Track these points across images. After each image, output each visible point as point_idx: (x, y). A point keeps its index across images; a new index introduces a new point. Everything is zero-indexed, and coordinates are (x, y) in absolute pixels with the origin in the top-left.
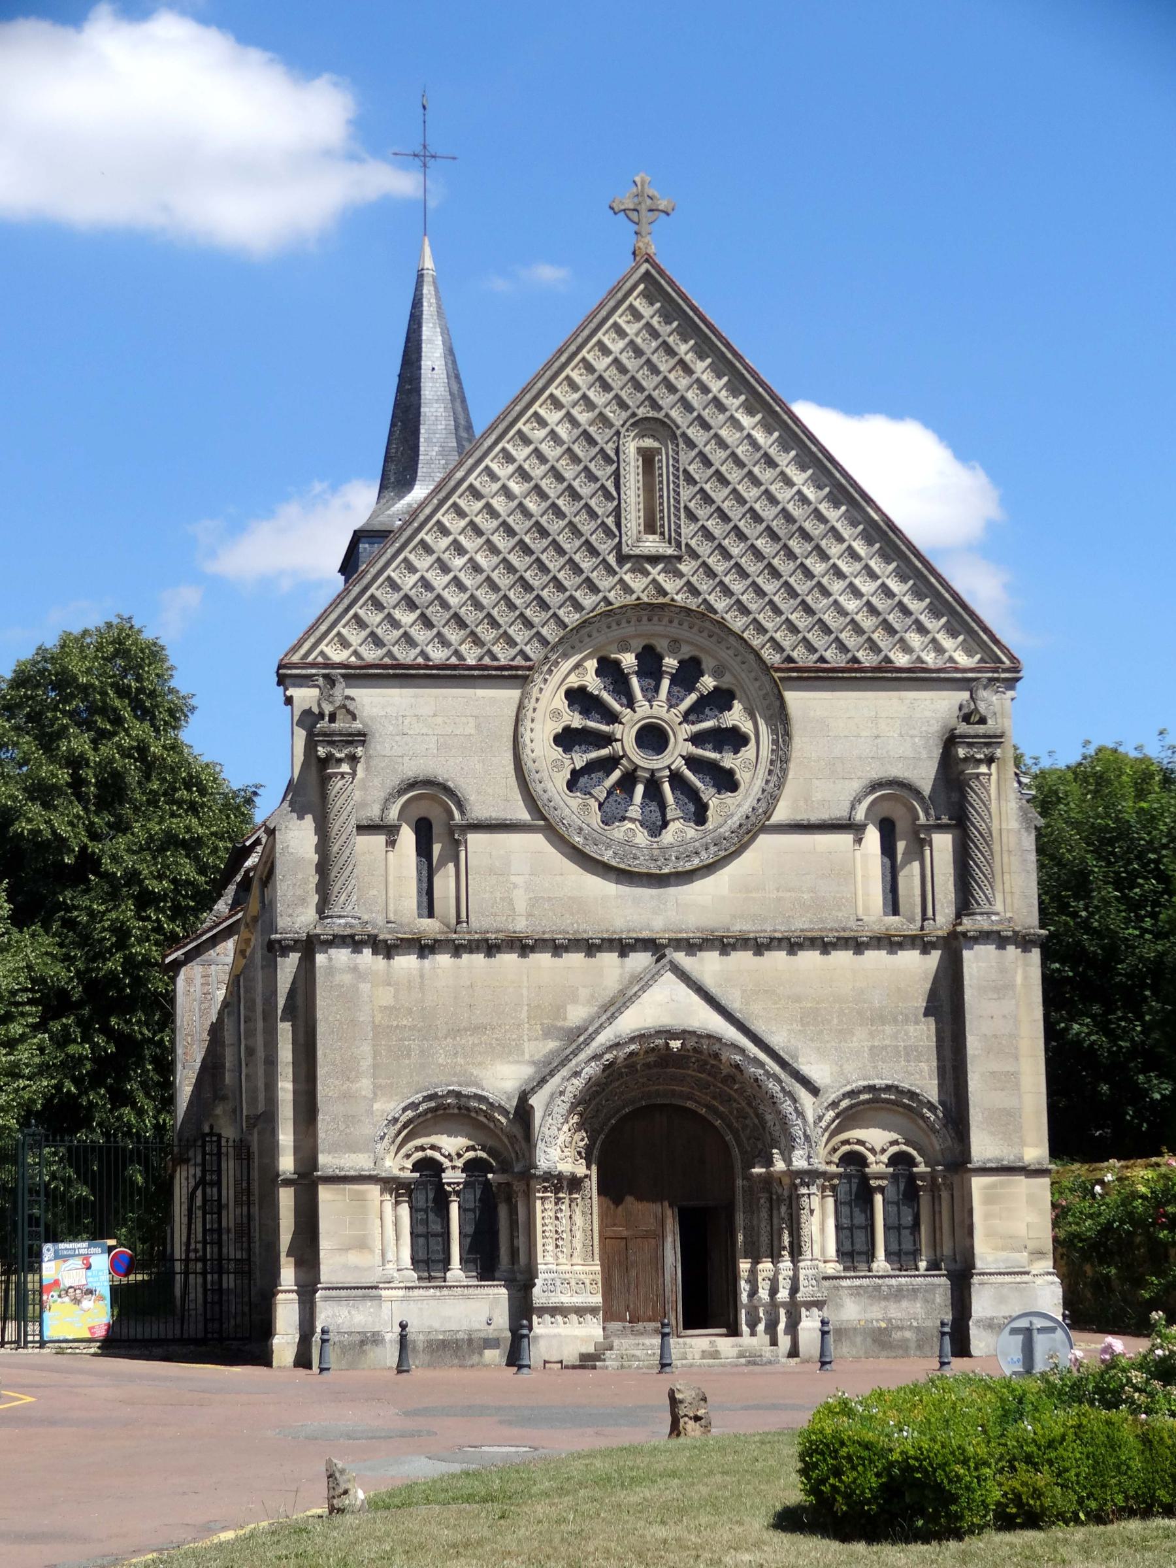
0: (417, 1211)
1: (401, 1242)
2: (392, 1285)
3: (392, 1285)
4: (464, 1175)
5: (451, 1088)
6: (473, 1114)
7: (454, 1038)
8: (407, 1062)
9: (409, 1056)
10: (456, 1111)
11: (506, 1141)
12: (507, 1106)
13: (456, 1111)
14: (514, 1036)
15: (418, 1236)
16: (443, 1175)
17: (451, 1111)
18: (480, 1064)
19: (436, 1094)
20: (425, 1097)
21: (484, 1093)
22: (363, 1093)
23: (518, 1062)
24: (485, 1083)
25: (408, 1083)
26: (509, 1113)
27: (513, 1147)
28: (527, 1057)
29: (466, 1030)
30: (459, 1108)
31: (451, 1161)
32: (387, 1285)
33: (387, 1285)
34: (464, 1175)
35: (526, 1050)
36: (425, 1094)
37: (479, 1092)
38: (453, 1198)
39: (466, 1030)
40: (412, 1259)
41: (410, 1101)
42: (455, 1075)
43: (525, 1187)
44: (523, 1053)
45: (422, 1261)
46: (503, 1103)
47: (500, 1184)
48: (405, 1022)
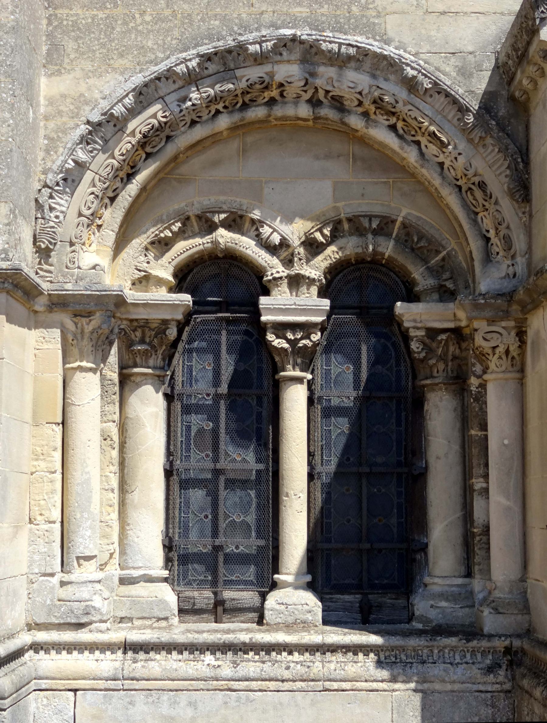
0: (187, 410)
1: (134, 497)
2: (84, 636)
3: (84, 636)
4: (326, 303)
5: (288, 32)
12: (459, 91)
13: (304, 111)
15: (185, 484)
16: (263, 300)
17: (290, 111)
19: (241, 47)
20: (207, 58)
21: (390, 50)
25: (159, 19)
26: (463, 110)
27: (475, 222)
30: (315, 103)
31: (288, 262)
32: (68, 636)
33: (68, 636)
34: (326, 303)
36: (206, 49)
37: (376, 46)
38: (291, 372)
40: (168, 547)
41: (162, 67)
45: (199, 558)
46: (446, 81)
47: (432, 333)
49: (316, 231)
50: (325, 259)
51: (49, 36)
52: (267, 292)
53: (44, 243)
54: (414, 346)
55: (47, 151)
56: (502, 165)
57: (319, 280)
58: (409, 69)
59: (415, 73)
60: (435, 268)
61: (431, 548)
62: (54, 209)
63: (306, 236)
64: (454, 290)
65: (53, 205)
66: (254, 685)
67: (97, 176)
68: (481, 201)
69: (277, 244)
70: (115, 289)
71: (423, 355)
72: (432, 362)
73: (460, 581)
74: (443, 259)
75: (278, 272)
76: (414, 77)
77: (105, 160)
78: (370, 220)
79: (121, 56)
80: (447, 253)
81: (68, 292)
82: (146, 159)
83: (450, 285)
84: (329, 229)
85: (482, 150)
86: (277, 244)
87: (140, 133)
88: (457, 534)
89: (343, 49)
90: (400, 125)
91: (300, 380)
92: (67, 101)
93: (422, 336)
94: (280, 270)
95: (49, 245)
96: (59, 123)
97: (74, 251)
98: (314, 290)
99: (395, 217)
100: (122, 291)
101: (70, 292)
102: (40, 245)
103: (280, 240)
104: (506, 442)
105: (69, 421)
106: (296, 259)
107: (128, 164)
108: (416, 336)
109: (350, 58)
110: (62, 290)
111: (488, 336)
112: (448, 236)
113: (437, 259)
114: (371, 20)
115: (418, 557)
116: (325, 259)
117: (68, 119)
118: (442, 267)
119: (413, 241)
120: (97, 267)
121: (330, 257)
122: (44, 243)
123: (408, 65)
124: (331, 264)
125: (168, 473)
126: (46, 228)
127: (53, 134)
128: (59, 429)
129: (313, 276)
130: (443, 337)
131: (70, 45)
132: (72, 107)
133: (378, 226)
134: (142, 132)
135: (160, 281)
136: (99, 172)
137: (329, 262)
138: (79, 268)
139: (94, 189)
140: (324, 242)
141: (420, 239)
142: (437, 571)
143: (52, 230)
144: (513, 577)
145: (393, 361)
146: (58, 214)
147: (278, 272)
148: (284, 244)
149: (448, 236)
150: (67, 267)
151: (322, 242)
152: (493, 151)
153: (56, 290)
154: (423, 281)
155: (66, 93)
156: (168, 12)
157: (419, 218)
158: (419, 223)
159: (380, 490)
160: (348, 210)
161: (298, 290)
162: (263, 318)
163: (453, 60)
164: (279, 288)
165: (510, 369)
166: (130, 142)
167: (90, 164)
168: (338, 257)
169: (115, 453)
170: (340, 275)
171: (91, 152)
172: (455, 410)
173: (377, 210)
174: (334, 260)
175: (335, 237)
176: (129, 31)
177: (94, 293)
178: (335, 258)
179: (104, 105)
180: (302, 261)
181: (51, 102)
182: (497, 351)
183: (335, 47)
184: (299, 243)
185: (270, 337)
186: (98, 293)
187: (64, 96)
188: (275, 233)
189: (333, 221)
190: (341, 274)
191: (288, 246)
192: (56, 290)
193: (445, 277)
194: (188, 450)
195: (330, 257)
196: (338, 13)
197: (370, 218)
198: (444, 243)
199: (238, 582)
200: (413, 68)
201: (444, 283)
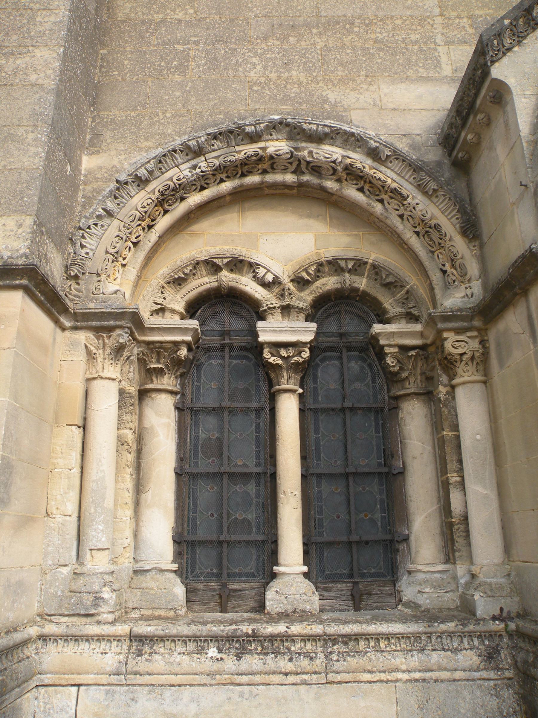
1: (148, 497)
6: (330, 184)
7: (285, 38)
8: (178, 78)
9: (183, 69)
10: (290, 178)
11: (415, 242)
14: (414, 37)
16: (260, 324)
18: (343, 81)
22: (33, 77)
23: (427, 79)
24: (355, 116)
28: (447, 71)
29: (308, 26)
34: (313, 326)
35: (444, 59)
39: (308, 26)
42: (286, 99)
43: (475, 345)
44: (438, 64)
47: (404, 349)
48: (180, 15)
49: (303, 270)
50: (311, 293)
51: (93, 129)
52: (262, 318)
53: (73, 271)
54: (389, 360)
55: (84, 206)
56: (453, 210)
57: (306, 310)
58: (372, 142)
59: (377, 144)
60: (401, 300)
61: (412, 538)
62: (85, 247)
63: (295, 275)
64: (419, 316)
65: (84, 244)
66: (257, 679)
67: (123, 223)
68: (437, 240)
69: (271, 281)
70: (131, 307)
71: (397, 369)
72: (405, 374)
73: (441, 567)
74: (407, 292)
75: (272, 304)
76: (377, 147)
77: (130, 211)
78: (346, 262)
79: (147, 139)
80: (411, 287)
81: (91, 311)
82: (163, 215)
83: (415, 312)
84: (313, 269)
85: (435, 200)
86: (271, 281)
87: (159, 191)
88: (435, 525)
89: (320, 128)
90: (366, 187)
91: (293, 391)
92: (103, 170)
93: (396, 352)
94: (274, 302)
95: (78, 273)
96: (95, 187)
97: (99, 281)
98: (302, 316)
99: (366, 260)
100: (137, 309)
101: (93, 311)
102: (70, 273)
103: (273, 278)
104: (478, 437)
105: (88, 427)
106: (286, 293)
107: (149, 217)
108: (390, 353)
109: (326, 135)
110: (86, 309)
111: (458, 344)
112: (410, 274)
113: (402, 292)
114: (340, 113)
115: (402, 547)
116: (311, 293)
117: (102, 183)
118: (407, 299)
119: (382, 277)
120: (118, 293)
121: (315, 292)
122: (73, 271)
123: (371, 139)
124: (316, 297)
125: (178, 475)
126: (77, 259)
127: (89, 194)
128: (77, 433)
129: (301, 306)
130: (413, 353)
131: (108, 134)
132: (106, 175)
133: (353, 266)
134: (161, 191)
135: (173, 311)
136: (124, 220)
137: (315, 295)
138: (103, 293)
139: (120, 233)
140: (310, 279)
141: (387, 276)
142: (420, 560)
143: (82, 261)
144: (496, 561)
145: (369, 379)
146: (88, 251)
147: (272, 304)
148: (276, 281)
149: (410, 274)
150: (93, 293)
151: (308, 280)
152: (444, 200)
153: (81, 309)
154: (393, 310)
155: (102, 165)
156: (183, 111)
157: (386, 261)
158: (386, 264)
159: (364, 489)
160: (328, 255)
161: (289, 318)
162: (261, 339)
163: (404, 140)
164: (273, 317)
165: (475, 373)
166: (150, 199)
167: (118, 214)
168: (321, 291)
169: (131, 457)
170: (323, 309)
171: (118, 204)
172: (426, 416)
173: (351, 254)
174: (318, 294)
175: (318, 277)
176: (154, 124)
177: (113, 311)
178: (319, 292)
179: (132, 169)
180: (292, 296)
181: (89, 172)
182: (465, 358)
183: (314, 127)
184: (289, 280)
185: (266, 354)
186: (116, 311)
187: (100, 168)
188: (269, 273)
189: (316, 263)
190: (324, 308)
191: (280, 283)
192: (81, 309)
193: (410, 306)
194: (196, 456)
195: (315, 292)
196: (314, 109)
197: (346, 260)
198: (407, 279)
199: (241, 575)
200: (375, 141)
201: (409, 310)
